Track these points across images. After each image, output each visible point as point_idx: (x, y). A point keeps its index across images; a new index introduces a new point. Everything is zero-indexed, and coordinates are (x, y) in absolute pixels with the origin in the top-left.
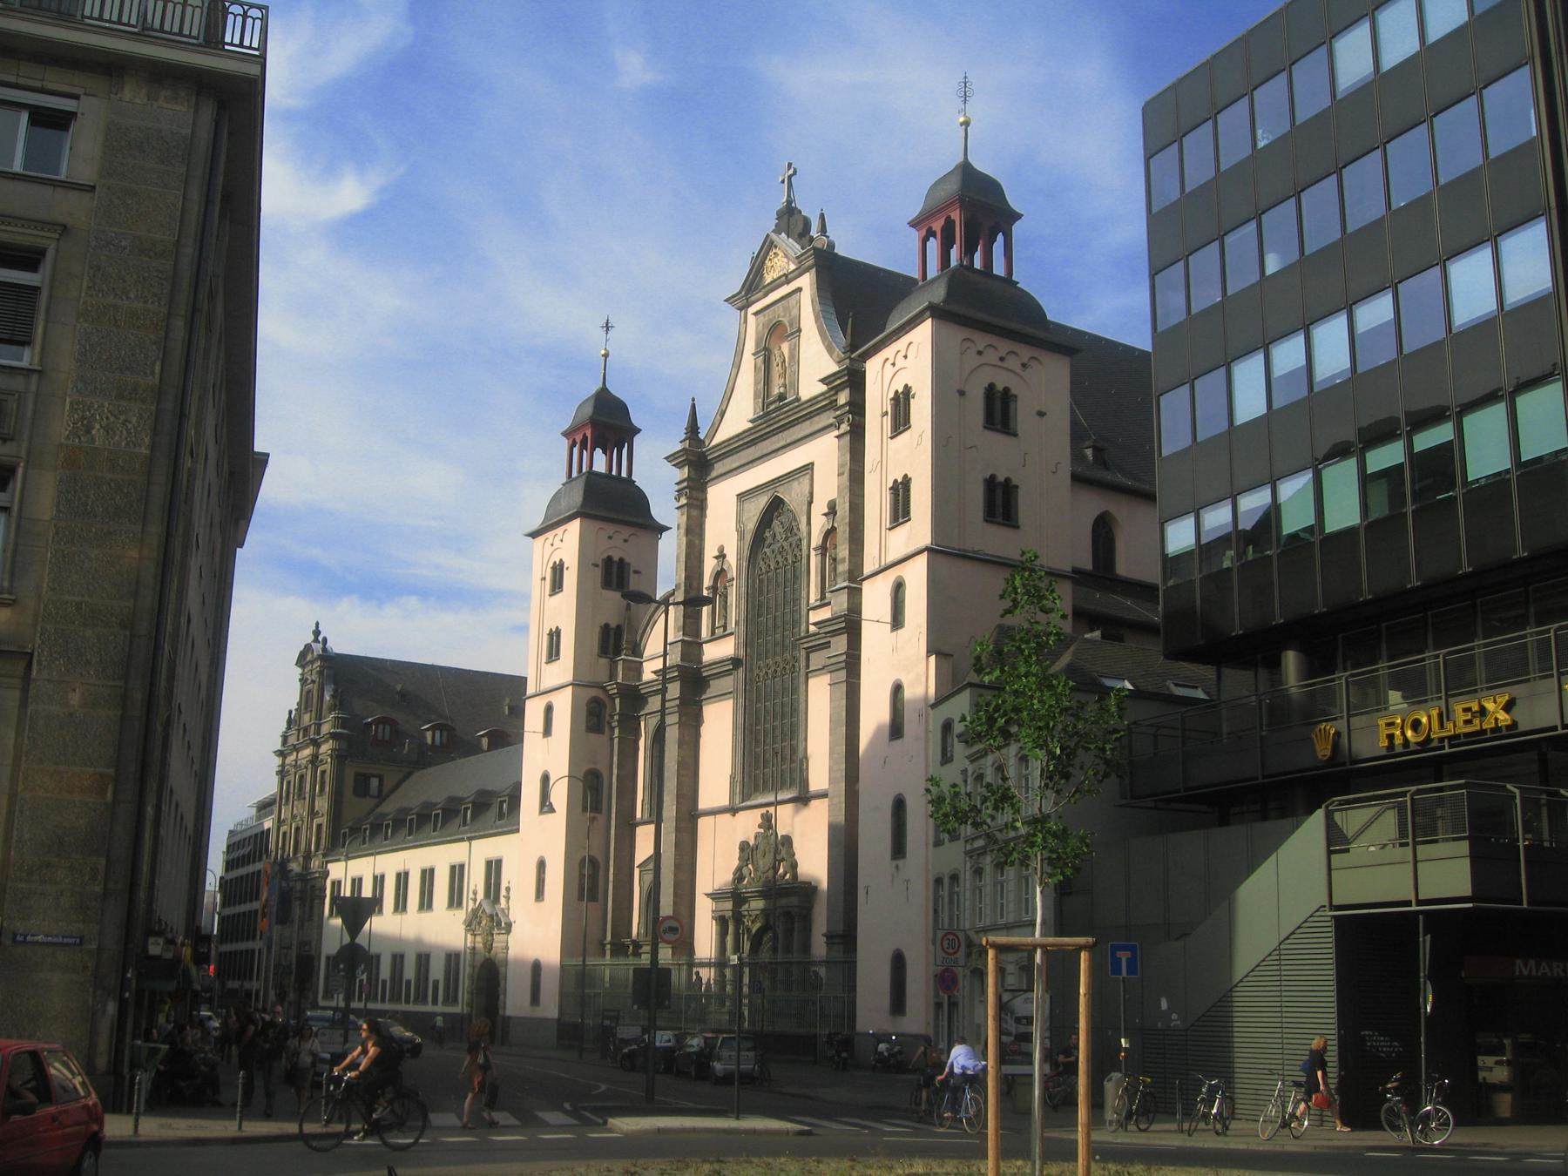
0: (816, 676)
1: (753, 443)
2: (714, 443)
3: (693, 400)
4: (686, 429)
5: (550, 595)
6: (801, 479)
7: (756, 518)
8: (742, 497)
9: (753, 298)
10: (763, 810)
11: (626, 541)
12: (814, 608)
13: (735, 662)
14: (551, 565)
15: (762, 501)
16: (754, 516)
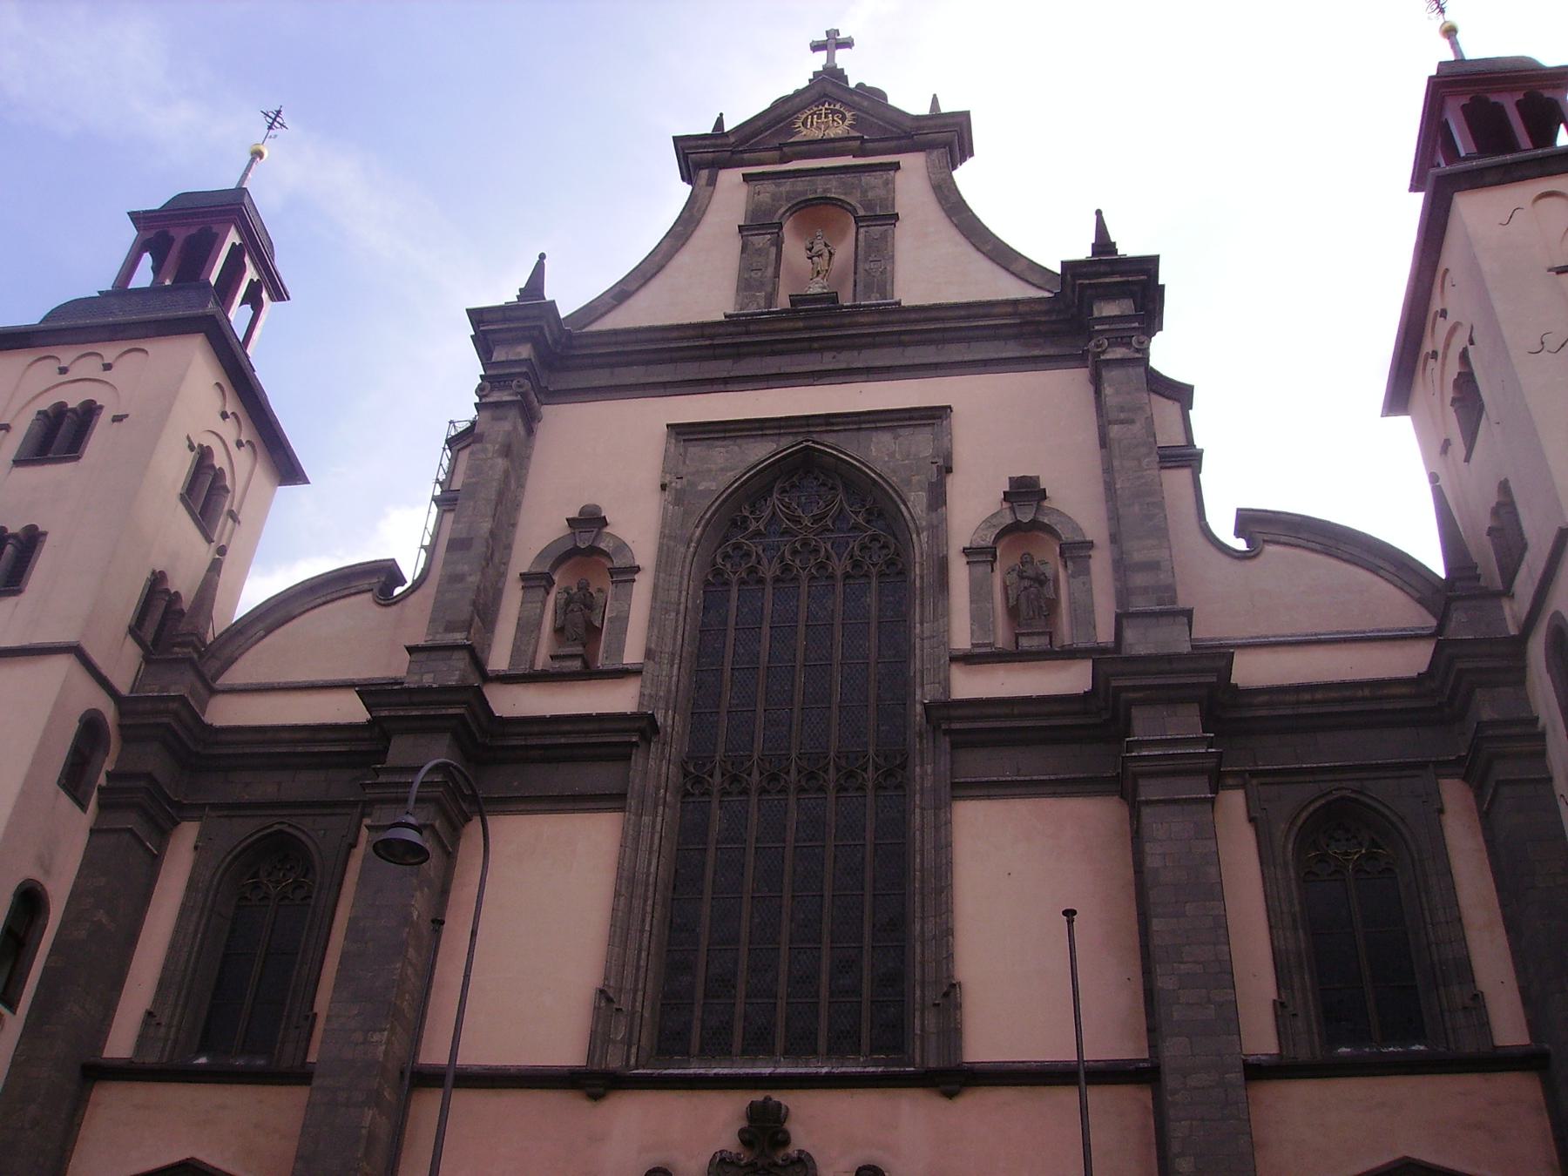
0: (989, 797)
1: (737, 352)
2: (595, 327)
3: (542, 256)
4: (520, 290)
5: (18, 462)
6: (901, 432)
7: (731, 476)
8: (683, 433)
9: (746, 156)
10: (758, 1096)
11: (239, 444)
12: (968, 659)
13: (642, 726)
14: (46, 404)
15: (760, 451)
16: (722, 470)
